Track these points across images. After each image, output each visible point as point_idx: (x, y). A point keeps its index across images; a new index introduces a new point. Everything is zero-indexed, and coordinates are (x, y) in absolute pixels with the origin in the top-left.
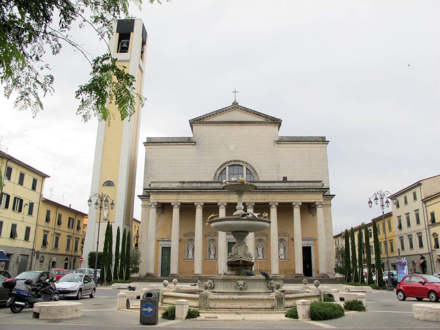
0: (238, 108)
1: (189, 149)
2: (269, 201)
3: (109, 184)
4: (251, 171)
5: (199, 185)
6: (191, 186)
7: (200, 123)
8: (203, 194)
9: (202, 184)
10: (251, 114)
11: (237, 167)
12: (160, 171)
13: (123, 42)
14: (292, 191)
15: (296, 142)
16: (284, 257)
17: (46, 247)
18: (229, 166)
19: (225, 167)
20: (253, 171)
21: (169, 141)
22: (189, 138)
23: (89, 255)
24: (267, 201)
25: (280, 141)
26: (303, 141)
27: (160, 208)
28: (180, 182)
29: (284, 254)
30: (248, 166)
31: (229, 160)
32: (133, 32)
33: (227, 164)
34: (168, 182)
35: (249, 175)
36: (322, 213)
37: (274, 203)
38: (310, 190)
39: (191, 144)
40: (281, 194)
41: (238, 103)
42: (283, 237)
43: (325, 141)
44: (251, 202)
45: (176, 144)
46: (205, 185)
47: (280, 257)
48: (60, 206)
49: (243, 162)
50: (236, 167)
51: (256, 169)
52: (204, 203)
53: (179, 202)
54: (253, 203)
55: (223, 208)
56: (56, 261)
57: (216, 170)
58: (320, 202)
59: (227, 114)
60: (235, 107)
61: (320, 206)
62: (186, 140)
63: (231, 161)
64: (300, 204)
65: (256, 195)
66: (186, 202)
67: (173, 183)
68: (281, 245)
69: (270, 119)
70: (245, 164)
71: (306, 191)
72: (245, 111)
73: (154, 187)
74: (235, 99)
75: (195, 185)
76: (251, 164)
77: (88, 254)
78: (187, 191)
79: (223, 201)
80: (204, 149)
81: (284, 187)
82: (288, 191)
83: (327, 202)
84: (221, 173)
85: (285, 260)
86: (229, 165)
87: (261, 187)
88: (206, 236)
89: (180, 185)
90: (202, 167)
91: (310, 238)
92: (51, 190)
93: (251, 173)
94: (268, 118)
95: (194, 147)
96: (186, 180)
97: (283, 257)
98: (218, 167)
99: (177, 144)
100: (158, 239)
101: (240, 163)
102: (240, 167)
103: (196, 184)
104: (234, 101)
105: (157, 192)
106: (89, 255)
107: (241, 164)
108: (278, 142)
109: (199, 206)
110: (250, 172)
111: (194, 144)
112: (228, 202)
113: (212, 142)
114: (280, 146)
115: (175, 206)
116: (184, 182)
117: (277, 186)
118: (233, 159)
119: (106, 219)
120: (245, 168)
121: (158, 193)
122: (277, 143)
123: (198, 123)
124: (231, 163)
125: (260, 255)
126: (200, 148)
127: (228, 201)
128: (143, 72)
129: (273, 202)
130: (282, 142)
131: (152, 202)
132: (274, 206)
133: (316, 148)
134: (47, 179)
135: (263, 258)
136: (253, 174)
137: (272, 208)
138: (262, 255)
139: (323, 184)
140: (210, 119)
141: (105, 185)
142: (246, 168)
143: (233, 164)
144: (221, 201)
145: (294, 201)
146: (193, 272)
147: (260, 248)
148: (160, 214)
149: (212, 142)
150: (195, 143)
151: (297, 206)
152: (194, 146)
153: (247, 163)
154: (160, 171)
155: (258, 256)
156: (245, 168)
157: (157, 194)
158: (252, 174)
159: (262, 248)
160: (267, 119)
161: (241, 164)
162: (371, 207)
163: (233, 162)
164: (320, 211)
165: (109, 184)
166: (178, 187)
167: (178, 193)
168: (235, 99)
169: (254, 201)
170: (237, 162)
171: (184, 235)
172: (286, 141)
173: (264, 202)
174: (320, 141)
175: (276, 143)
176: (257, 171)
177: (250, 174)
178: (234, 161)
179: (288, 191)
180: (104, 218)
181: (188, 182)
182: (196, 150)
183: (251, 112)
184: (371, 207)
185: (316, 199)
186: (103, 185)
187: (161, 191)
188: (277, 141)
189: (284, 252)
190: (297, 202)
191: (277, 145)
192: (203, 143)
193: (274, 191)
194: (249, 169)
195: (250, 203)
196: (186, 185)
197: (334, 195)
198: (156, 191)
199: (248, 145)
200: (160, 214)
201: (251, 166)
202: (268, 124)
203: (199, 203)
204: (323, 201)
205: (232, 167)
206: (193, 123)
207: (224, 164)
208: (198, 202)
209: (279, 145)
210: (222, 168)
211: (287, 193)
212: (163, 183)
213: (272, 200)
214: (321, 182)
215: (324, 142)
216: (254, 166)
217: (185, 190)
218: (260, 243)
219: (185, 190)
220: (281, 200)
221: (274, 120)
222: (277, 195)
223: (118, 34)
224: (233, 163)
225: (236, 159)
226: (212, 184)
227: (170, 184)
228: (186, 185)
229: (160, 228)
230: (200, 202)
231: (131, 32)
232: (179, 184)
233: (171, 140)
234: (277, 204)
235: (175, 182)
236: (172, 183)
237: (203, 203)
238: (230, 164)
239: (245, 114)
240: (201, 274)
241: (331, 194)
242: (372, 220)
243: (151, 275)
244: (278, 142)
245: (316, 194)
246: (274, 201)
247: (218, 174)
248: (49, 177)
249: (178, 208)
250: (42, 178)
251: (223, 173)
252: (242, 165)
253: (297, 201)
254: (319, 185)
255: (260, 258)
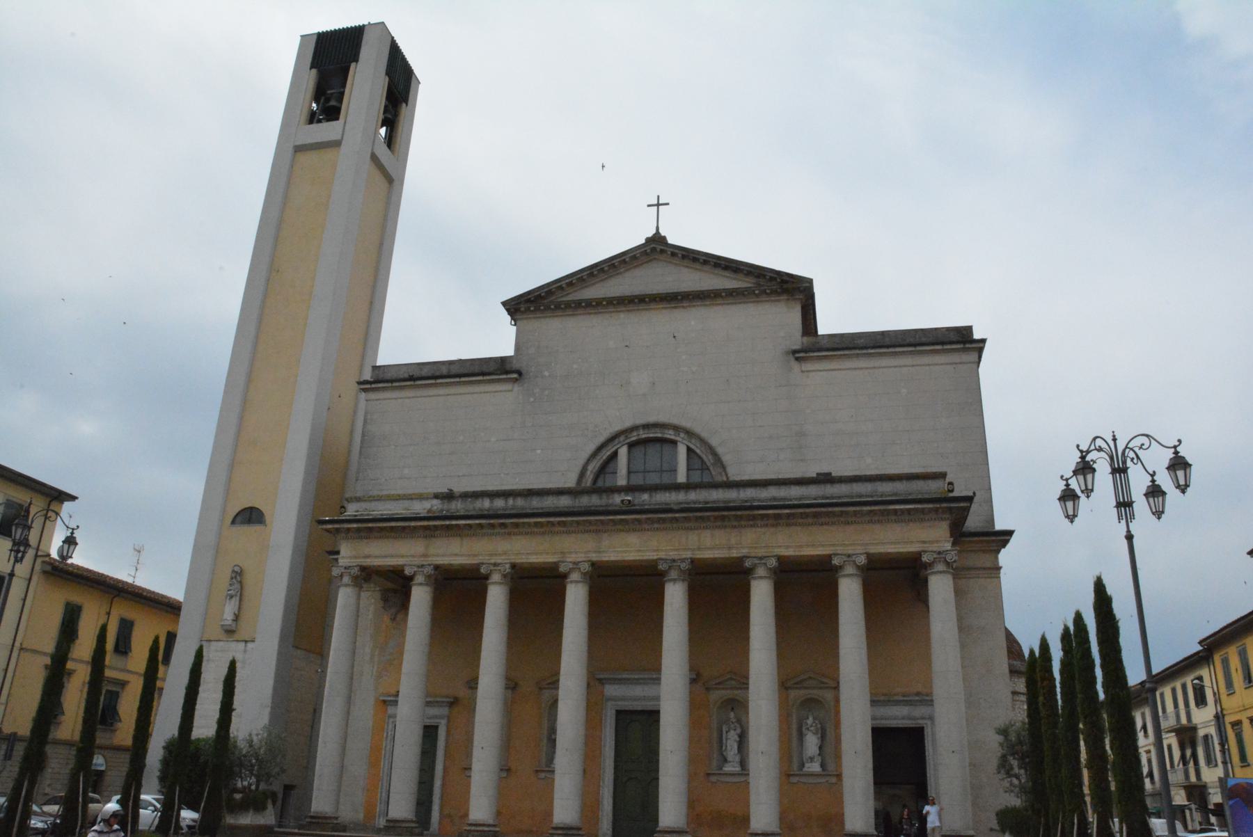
0: (662, 251)
1: (502, 396)
2: (744, 552)
3: (251, 516)
4: (704, 457)
5: (499, 503)
6: (474, 509)
7: (537, 310)
8: (509, 534)
9: (511, 501)
10: (706, 268)
11: (658, 446)
12: (406, 471)
13: (332, 94)
14: (828, 514)
15: (865, 351)
16: (823, 765)
17: (116, 731)
18: (631, 446)
19: (614, 449)
20: (710, 457)
21: (438, 374)
22: (503, 361)
23: (164, 748)
24: (735, 555)
25: (806, 351)
26: (888, 347)
27: (395, 591)
28: (436, 496)
29: (819, 755)
30: (693, 441)
31: (628, 424)
32: (357, 61)
33: (622, 438)
34: (399, 495)
35: (699, 472)
36: (951, 595)
37: (761, 558)
38: (897, 507)
39: (504, 376)
40: (788, 525)
41: (664, 238)
42: (815, 693)
43: (969, 339)
44: (676, 557)
45: (458, 380)
46: (520, 502)
47: (807, 765)
48: (122, 594)
49: (676, 428)
50: (652, 450)
51: (720, 450)
52: (513, 566)
53: (430, 563)
54: (683, 560)
55: (577, 582)
56: (103, 768)
57: (581, 462)
58: (939, 553)
59: (627, 274)
60: (654, 250)
61: (940, 567)
62: (492, 368)
63: (634, 428)
64: (862, 560)
65: (696, 532)
66: (452, 562)
67: (415, 502)
68: (810, 721)
69: (772, 279)
70: (682, 435)
71: (883, 513)
72: (685, 261)
73: (356, 516)
74: (657, 228)
75: (486, 503)
76: (704, 435)
77: (164, 744)
78: (454, 522)
79: (580, 557)
80: (547, 392)
81: (800, 499)
82: (816, 515)
83: (982, 560)
84: (602, 470)
85: (823, 780)
86: (628, 441)
87: (714, 502)
88: (540, 689)
89: (436, 504)
90: (539, 451)
91: (918, 694)
92: (139, 552)
93: (704, 468)
94: (764, 276)
95: (516, 388)
96: (460, 487)
97: (815, 767)
98: (591, 447)
99: (463, 379)
100: (381, 698)
101: (666, 431)
102: (667, 448)
103: (492, 502)
104: (654, 231)
105: (358, 530)
106: (164, 748)
107: (668, 436)
108: (797, 355)
109: (496, 577)
110: (703, 461)
111: (515, 376)
112: (594, 559)
113: (575, 366)
114: (808, 366)
115: (416, 578)
116: (449, 496)
117: (775, 499)
118: (639, 421)
119: (229, 628)
120: (682, 451)
121: (363, 534)
122: (797, 359)
123: (532, 309)
124: (635, 434)
125: (730, 759)
126: (537, 390)
127: (594, 557)
128: (396, 183)
129: (760, 555)
130: (812, 354)
131: (344, 565)
132: (761, 571)
133: (939, 366)
134: (67, 506)
135: (742, 770)
136: (711, 468)
137: (755, 578)
138: (737, 759)
139: (950, 483)
140: (571, 295)
141: (239, 519)
142: (689, 449)
143: (644, 436)
144: (571, 558)
145: (839, 550)
146: (466, 815)
147: (732, 732)
148: (393, 610)
149: (575, 366)
150: (520, 373)
151: (850, 570)
152: (516, 385)
153: (689, 433)
154: (406, 471)
155: (725, 760)
156: (682, 451)
157: (361, 538)
158: (708, 469)
159: (739, 731)
160: (762, 281)
161: (670, 435)
162: (1071, 518)
163: (641, 432)
164: (940, 588)
165: (251, 516)
166: (429, 511)
167: (428, 532)
168: (657, 228)
169: (688, 555)
170: (658, 430)
171: (468, 682)
172: (828, 350)
173: (727, 556)
174: (954, 340)
175: (792, 359)
176: (726, 459)
177: (702, 469)
178: (647, 426)
179: (816, 515)
180: (225, 628)
181: (465, 496)
182: (521, 397)
183: (705, 262)
184: (1071, 518)
185: (924, 542)
186: (233, 522)
187: (370, 525)
188: (794, 352)
189: (820, 748)
190: (849, 556)
191: (796, 366)
192: (546, 374)
193: (763, 517)
194: (698, 451)
195: (674, 561)
196: (457, 506)
197: (1010, 533)
198: (355, 525)
199: (694, 369)
200: (393, 610)
201: (703, 441)
202: (764, 298)
203: (495, 565)
204: (949, 548)
205: (639, 451)
206: (519, 307)
207: (611, 439)
208: (493, 561)
209: (803, 364)
210: (606, 453)
211: (810, 520)
212: (383, 503)
213: (756, 548)
214: (943, 476)
215: (967, 346)
216: (714, 442)
217: (447, 523)
218: (732, 715)
219: (447, 523)
220: (788, 547)
221: (783, 282)
222: (773, 530)
223: (314, 71)
224: (644, 435)
225: (652, 419)
226: (545, 498)
227: (406, 503)
228: (456, 505)
229: (395, 659)
230: (499, 561)
231: (351, 62)
232: (435, 502)
233: (444, 371)
234: (773, 563)
235: (421, 497)
236: (412, 499)
237: (508, 566)
238: (634, 437)
239: (685, 270)
240: (491, 822)
241: (999, 526)
242: (1200, 643)
243: (320, 821)
244: (797, 355)
245: (922, 520)
246: (761, 552)
247: (589, 473)
248: (73, 498)
249: (427, 585)
250: (48, 500)
251: (610, 468)
252: (673, 437)
253: (850, 552)
254: (934, 487)
255: (728, 768)
